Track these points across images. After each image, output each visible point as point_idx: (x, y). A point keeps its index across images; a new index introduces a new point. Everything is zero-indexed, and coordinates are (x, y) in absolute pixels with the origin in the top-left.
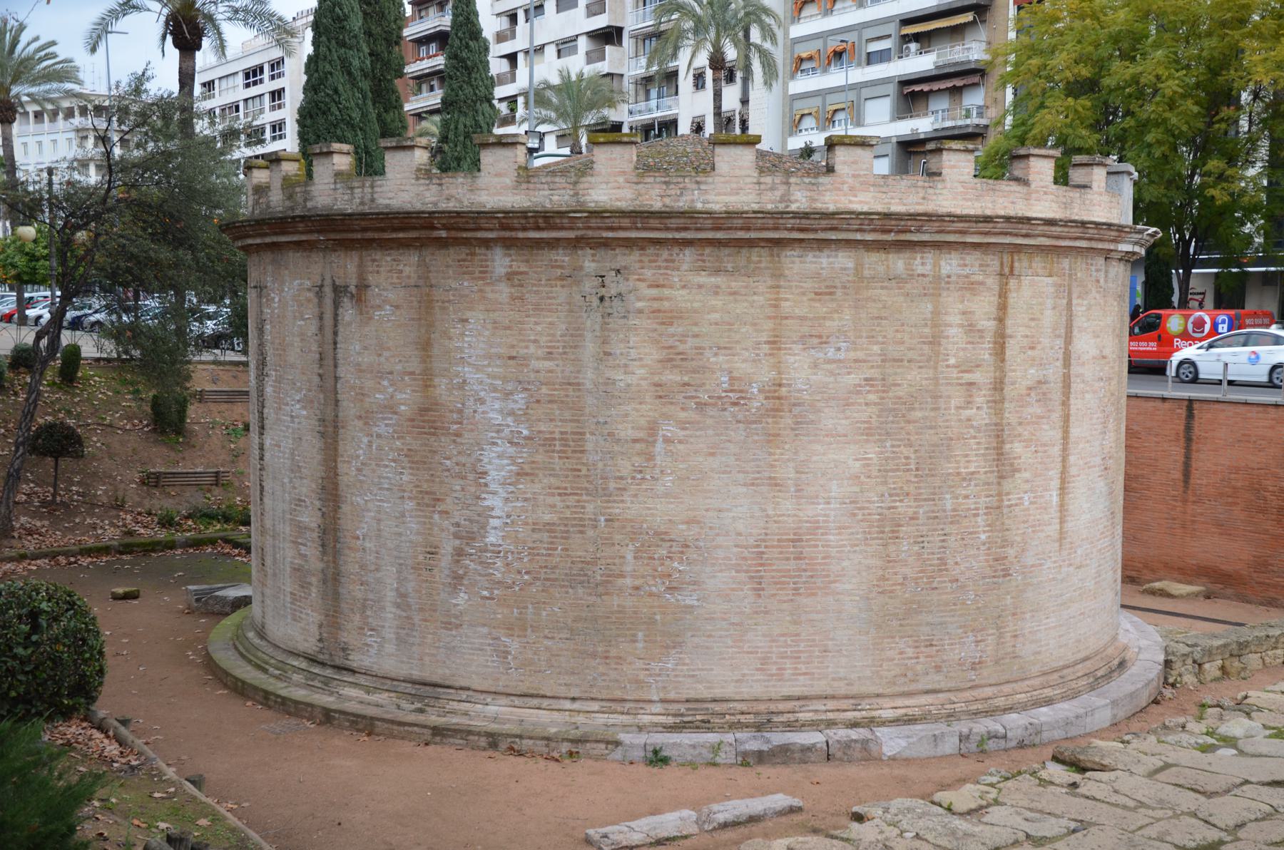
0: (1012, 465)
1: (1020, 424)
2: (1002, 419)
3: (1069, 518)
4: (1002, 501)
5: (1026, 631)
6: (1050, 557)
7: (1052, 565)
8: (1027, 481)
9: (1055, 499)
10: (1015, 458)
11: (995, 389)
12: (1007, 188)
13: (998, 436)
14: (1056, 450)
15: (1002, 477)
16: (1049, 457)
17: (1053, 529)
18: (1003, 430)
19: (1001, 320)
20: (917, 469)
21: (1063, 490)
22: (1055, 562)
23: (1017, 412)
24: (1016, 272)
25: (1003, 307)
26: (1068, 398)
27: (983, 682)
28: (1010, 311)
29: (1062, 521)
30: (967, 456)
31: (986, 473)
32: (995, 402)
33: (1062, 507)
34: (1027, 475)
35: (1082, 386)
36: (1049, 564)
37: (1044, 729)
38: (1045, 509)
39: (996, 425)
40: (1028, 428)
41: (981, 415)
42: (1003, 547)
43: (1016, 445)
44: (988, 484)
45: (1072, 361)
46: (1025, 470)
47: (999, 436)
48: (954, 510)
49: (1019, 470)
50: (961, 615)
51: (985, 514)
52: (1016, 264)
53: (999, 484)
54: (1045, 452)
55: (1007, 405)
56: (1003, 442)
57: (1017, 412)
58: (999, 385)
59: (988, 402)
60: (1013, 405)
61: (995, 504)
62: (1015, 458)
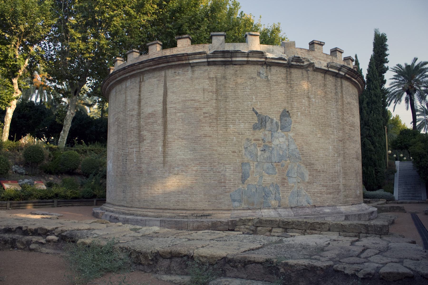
0: (143, 138)
1: (146, 125)
2: (140, 124)
3: (169, 156)
4: (140, 149)
5: (149, 193)
6: (159, 169)
7: (160, 172)
8: (148, 143)
9: (160, 149)
10: (144, 136)
11: (138, 116)
12: (142, 57)
13: (139, 130)
14: (161, 133)
15: (141, 142)
16: (157, 135)
17: (161, 159)
18: (140, 128)
19: (140, 95)
20: (122, 141)
21: (164, 145)
22: (161, 171)
23: (145, 122)
24: (144, 80)
25: (140, 91)
26: (166, 116)
27: (135, 206)
28: (142, 92)
29: (164, 157)
30: (131, 136)
31: (135, 141)
32: (138, 119)
33: (164, 152)
34: (149, 141)
35: (175, 111)
36: (158, 171)
37: (129, 220)
38: (156, 152)
39: (138, 126)
40: (149, 126)
41: (134, 124)
42: (140, 164)
43: (144, 132)
44: (136, 144)
45: (167, 103)
46: (148, 140)
47: (139, 129)
48: (128, 152)
49: (145, 140)
50: (130, 184)
51: (135, 153)
52: (144, 78)
53: (139, 144)
54: (155, 133)
55: (141, 120)
56: (140, 131)
57: (145, 122)
58: (139, 114)
59: (136, 120)
60: (143, 120)
61: (138, 150)
62: (144, 136)
